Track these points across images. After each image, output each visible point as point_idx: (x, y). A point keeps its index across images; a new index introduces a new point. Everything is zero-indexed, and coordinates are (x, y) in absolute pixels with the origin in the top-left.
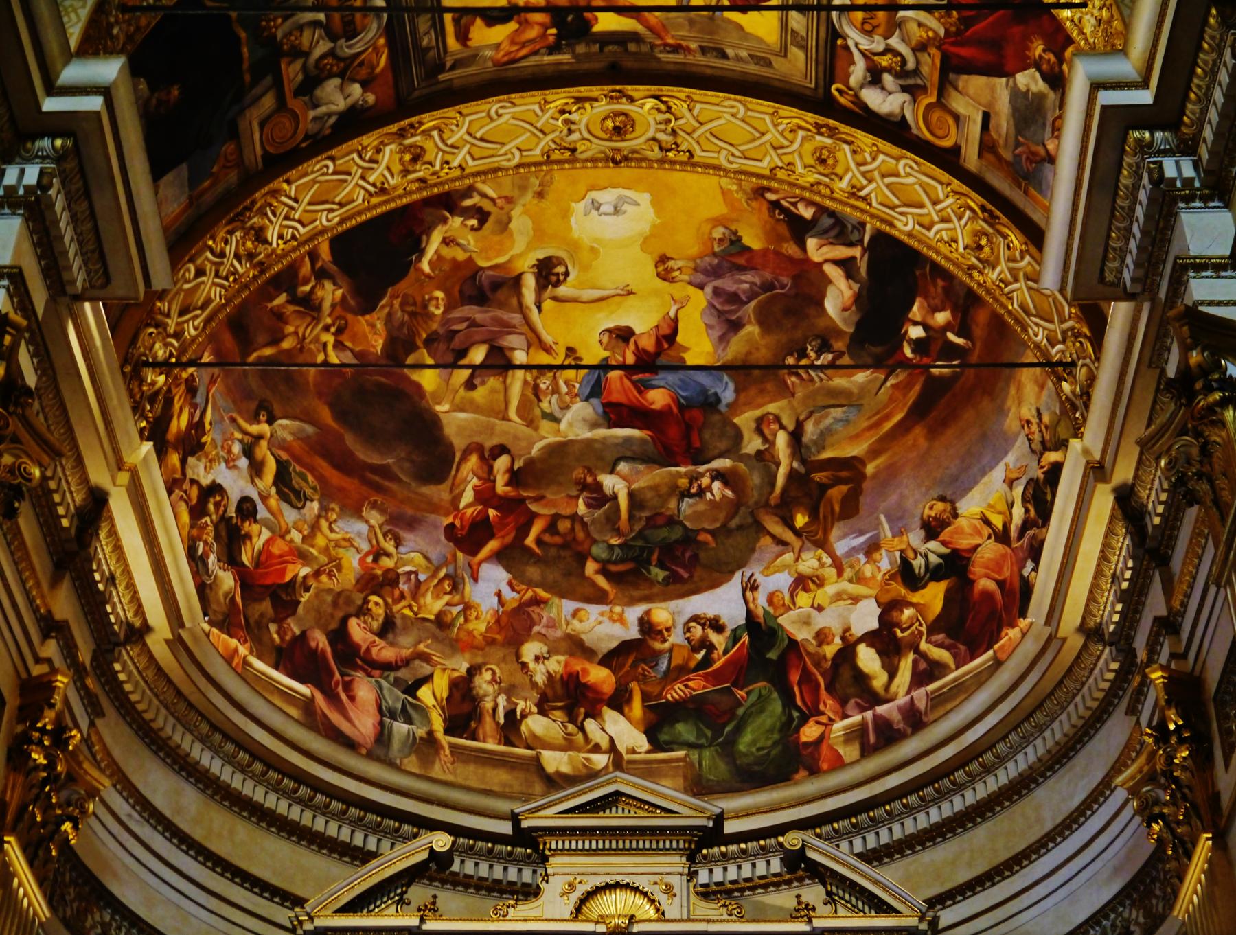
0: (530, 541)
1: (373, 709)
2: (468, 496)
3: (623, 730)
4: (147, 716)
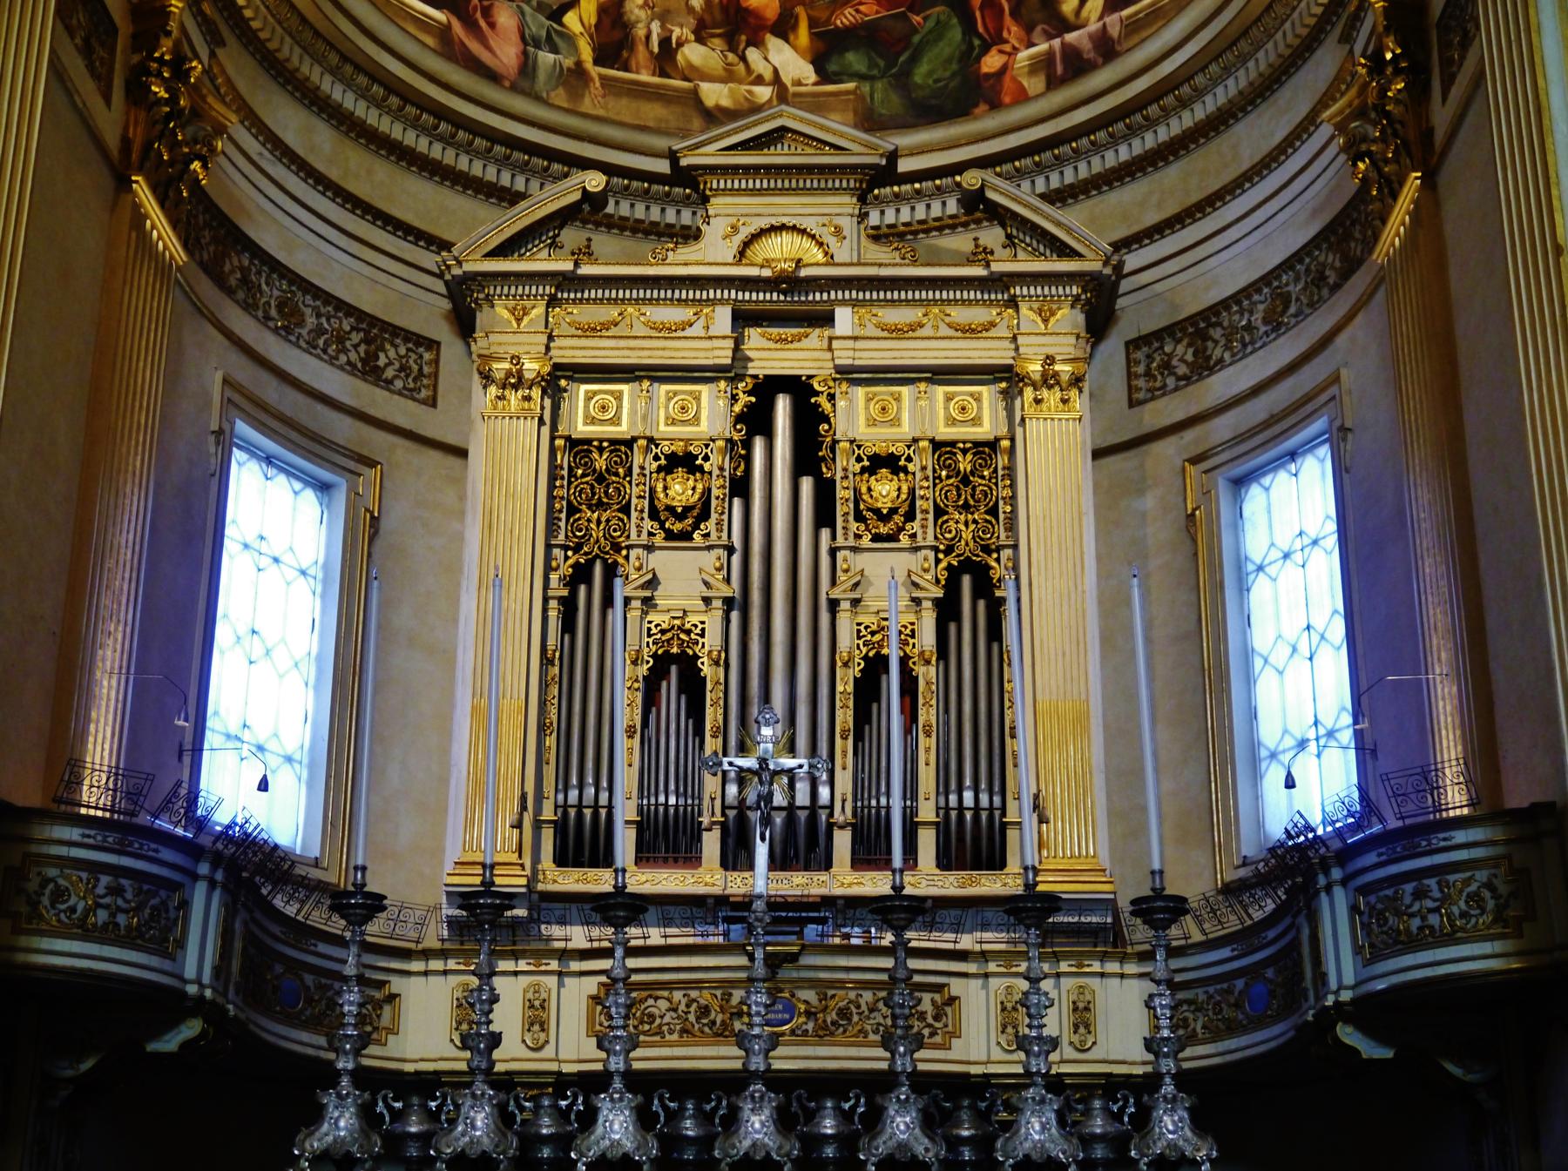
1: (515, 37)
3: (787, 60)
4: (272, 46)
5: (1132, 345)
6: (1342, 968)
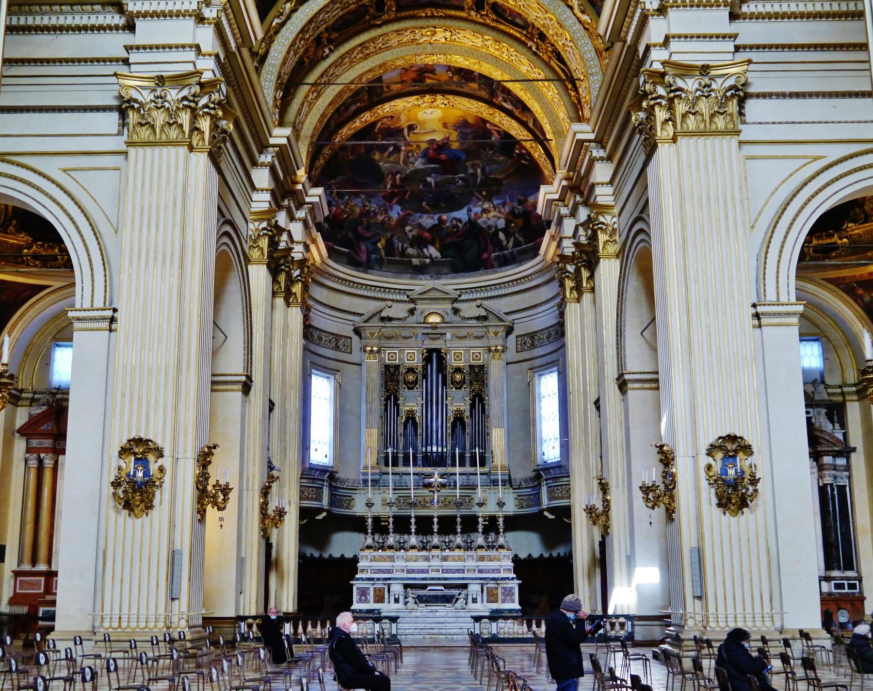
0: (407, 197)
2: (389, 186)
5: (517, 337)
6: (545, 502)
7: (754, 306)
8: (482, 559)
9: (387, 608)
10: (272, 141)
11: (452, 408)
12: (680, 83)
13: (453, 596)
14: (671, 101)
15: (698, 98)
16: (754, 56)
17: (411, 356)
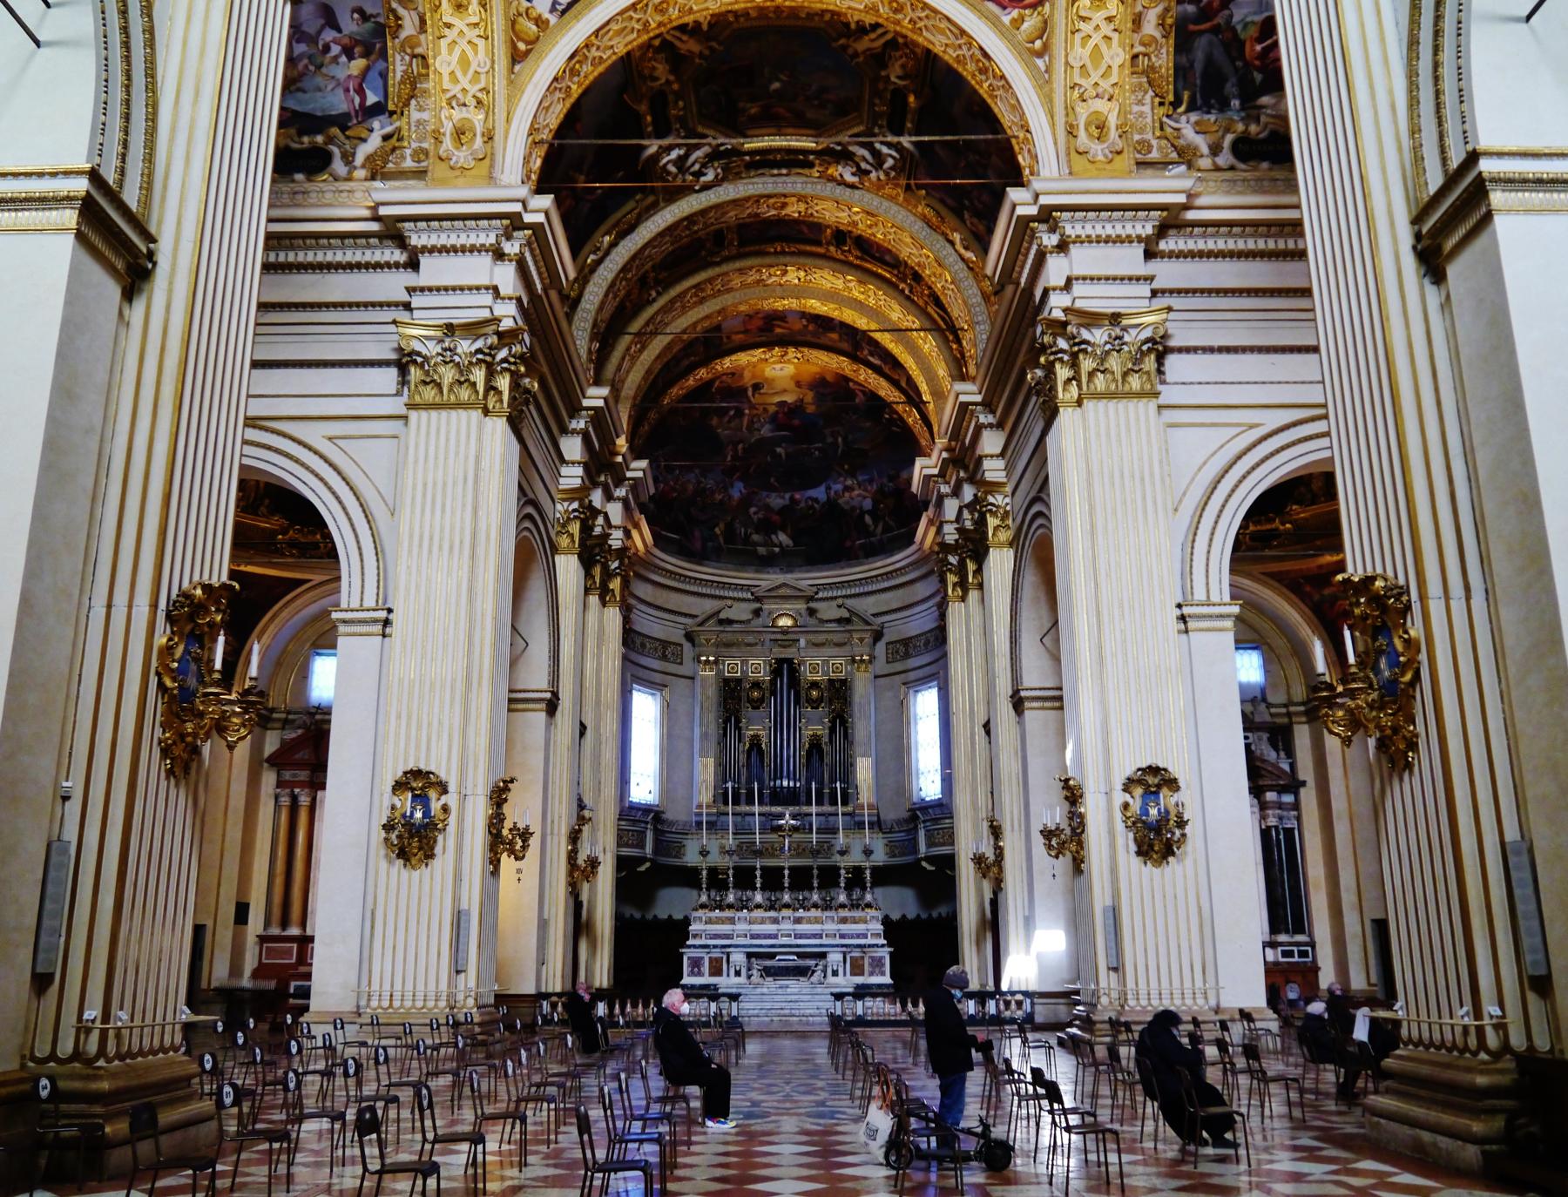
3: (783, 538)
6: (923, 848)
7: (1179, 606)
8: (844, 920)
9: (726, 982)
10: (586, 403)
11: (807, 733)
12: (1085, 335)
13: (809, 968)
14: (1074, 356)
15: (1108, 353)
16: (1176, 302)
17: (757, 667)
